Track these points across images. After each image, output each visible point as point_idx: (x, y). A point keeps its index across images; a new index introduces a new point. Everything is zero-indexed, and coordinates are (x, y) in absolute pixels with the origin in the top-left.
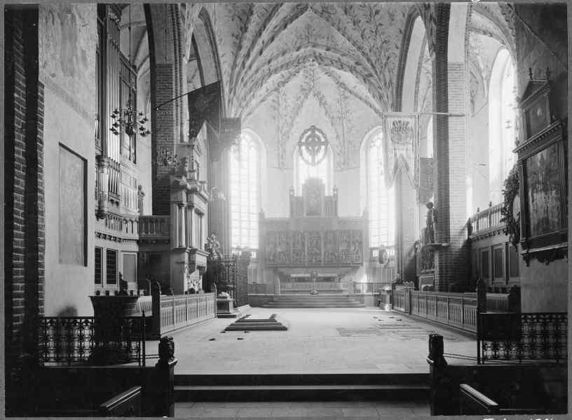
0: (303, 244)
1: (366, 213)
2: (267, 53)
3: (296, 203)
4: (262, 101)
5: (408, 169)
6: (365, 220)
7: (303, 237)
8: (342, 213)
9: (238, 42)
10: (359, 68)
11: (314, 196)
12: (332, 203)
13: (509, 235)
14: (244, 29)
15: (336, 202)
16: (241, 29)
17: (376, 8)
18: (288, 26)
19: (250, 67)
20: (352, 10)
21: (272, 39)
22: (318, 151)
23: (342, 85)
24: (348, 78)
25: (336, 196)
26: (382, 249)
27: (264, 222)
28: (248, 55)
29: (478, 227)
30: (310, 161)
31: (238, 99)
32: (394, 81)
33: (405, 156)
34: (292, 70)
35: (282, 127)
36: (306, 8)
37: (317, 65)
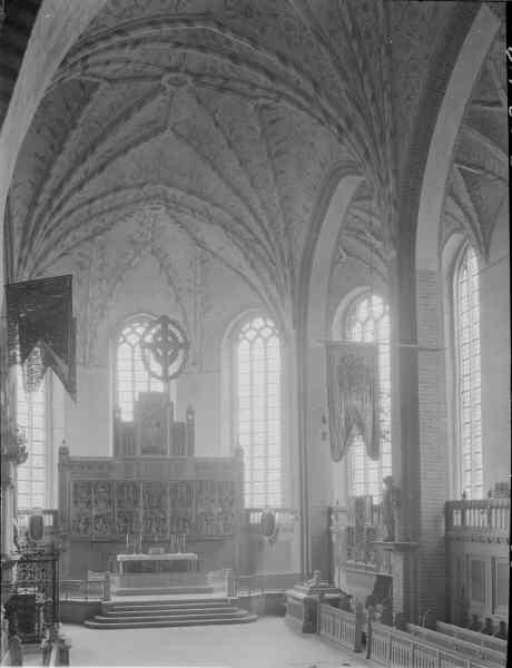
0: (136, 502)
1: (239, 452)
2: (90, 190)
3: (124, 437)
6: (235, 463)
7: (136, 491)
8: (203, 449)
9: (44, 168)
10: (240, 227)
11: (154, 422)
12: (183, 435)
14: (58, 149)
15: (192, 435)
16: (52, 147)
18: (132, 151)
19: (59, 208)
21: (102, 168)
22: (173, 358)
23: (200, 243)
24: (213, 237)
25: (191, 424)
26: (266, 511)
27: (66, 463)
28: (56, 192)
30: (160, 374)
31: (34, 257)
32: (298, 257)
33: (359, 410)
34: (121, 213)
35: (93, 298)
36: (162, 130)
37: (164, 209)
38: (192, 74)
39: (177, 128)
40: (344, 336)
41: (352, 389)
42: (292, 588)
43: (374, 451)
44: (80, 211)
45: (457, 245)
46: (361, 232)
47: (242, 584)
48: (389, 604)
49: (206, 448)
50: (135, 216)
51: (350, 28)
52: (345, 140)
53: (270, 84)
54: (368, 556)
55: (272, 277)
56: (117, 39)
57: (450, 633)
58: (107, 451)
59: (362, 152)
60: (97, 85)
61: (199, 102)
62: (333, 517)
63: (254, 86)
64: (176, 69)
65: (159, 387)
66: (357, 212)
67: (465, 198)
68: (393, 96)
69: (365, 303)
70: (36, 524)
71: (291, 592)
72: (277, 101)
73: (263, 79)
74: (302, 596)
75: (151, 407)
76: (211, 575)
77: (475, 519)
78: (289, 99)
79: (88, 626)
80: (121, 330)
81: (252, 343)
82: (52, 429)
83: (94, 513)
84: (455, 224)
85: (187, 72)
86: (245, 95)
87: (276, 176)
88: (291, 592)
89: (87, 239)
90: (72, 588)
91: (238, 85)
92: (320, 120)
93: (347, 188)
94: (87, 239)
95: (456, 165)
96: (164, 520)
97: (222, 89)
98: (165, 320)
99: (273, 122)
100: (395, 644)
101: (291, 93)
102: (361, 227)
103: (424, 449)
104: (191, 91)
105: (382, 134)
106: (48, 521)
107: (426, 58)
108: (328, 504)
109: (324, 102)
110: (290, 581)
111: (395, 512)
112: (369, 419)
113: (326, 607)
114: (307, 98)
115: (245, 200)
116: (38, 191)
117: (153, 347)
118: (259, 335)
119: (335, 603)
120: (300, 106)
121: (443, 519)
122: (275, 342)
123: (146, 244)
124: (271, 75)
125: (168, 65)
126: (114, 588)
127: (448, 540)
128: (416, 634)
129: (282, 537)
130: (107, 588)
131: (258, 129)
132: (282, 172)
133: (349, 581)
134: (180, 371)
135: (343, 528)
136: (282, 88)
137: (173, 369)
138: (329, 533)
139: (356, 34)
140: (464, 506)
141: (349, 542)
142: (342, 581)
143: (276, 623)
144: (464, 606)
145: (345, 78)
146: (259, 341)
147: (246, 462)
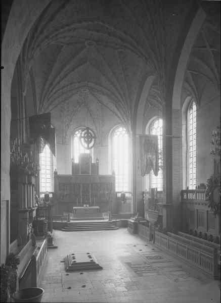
1: (113, 173)
2: (62, 83)
4: (56, 107)
12: (95, 167)
15: (98, 167)
19: (51, 91)
24: (104, 99)
27: (57, 177)
28: (51, 84)
37: (88, 91)
40: (150, 133)
42: (130, 219)
43: (156, 174)
44: (59, 92)
45: (189, 101)
46: (155, 97)
47: (114, 217)
48: (162, 226)
49: (102, 172)
50: (79, 93)
52: (148, 63)
54: (156, 208)
55: (124, 113)
56: (67, 28)
57: (182, 236)
58: (70, 173)
60: (62, 46)
62: (144, 195)
65: (88, 152)
66: (153, 89)
67: (192, 84)
69: (157, 122)
70: (47, 196)
71: (130, 220)
74: (133, 221)
75: (85, 159)
76: (103, 214)
77: (191, 196)
79: (63, 231)
80: (75, 132)
81: (119, 136)
82: (53, 165)
83: (65, 193)
84: (188, 93)
88: (130, 220)
89: (62, 101)
90: (58, 218)
93: (150, 80)
94: (62, 101)
95: (188, 71)
96: (89, 196)
98: (88, 129)
100: (162, 239)
102: (156, 95)
103: (174, 172)
106: (51, 196)
108: (143, 191)
110: (130, 216)
112: (154, 162)
113: (140, 226)
115: (115, 86)
116: (44, 85)
117: (84, 137)
118: (121, 134)
119: (143, 224)
120: (132, 51)
121: (180, 196)
122: (127, 135)
123: (82, 103)
124: (122, 40)
126: (71, 218)
128: (170, 236)
129: (128, 201)
130: (69, 218)
133: (149, 217)
134: (94, 145)
135: (147, 199)
137: (91, 145)
140: (188, 191)
142: (147, 216)
143: (125, 230)
146: (121, 135)
147: (116, 176)
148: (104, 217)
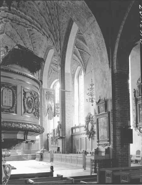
5: (52, 109)
13: (87, 135)
17: (34, 41)
20: (24, 39)
29: (75, 131)
36: (4, 33)
38: (10, 19)
39: (7, 33)
41: (49, 99)
51: (49, 13)
52: (49, 40)
53: (30, 24)
59: (53, 43)
61: (13, 27)
62: (49, 136)
63: (26, 24)
64: (6, 18)
66: (54, 59)
68: (59, 30)
72: (33, 29)
73: (28, 23)
76: (17, 150)
77: (77, 130)
78: (35, 28)
85: (9, 18)
86: (25, 27)
87: (34, 48)
91: (22, 24)
92: (43, 34)
97: (19, 24)
99: (32, 34)
101: (35, 27)
104: (10, 23)
105: (57, 39)
107: (67, 22)
109: (43, 30)
111: (60, 129)
112: (54, 107)
114: (39, 28)
120: (38, 31)
125: (4, 16)
127: (72, 136)
131: (29, 36)
132: (35, 47)
136: (33, 25)
138: (48, 140)
139: (50, 14)
140: (75, 128)
141: (52, 141)
144: (75, 150)
145: (48, 24)
148: (18, 153)
